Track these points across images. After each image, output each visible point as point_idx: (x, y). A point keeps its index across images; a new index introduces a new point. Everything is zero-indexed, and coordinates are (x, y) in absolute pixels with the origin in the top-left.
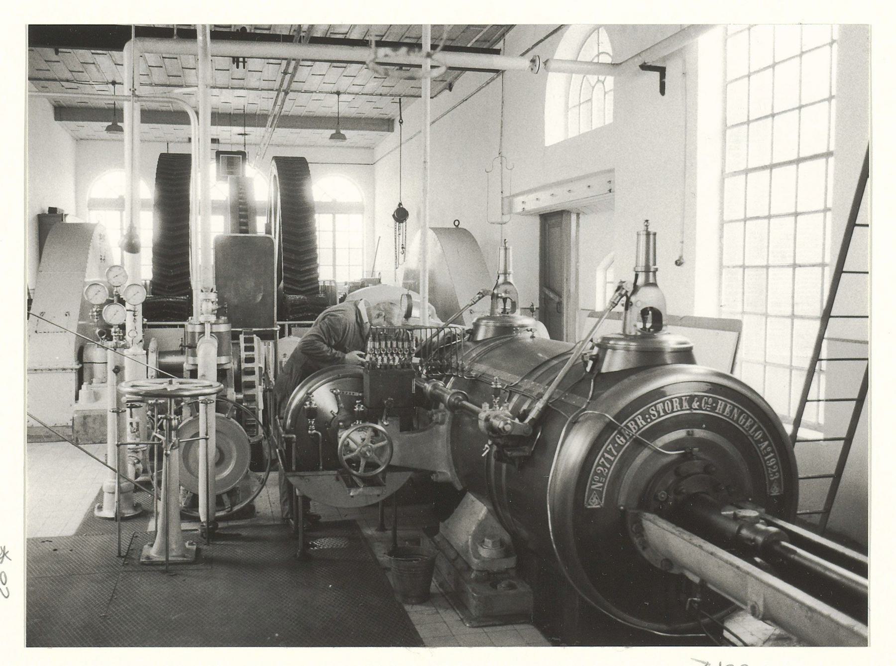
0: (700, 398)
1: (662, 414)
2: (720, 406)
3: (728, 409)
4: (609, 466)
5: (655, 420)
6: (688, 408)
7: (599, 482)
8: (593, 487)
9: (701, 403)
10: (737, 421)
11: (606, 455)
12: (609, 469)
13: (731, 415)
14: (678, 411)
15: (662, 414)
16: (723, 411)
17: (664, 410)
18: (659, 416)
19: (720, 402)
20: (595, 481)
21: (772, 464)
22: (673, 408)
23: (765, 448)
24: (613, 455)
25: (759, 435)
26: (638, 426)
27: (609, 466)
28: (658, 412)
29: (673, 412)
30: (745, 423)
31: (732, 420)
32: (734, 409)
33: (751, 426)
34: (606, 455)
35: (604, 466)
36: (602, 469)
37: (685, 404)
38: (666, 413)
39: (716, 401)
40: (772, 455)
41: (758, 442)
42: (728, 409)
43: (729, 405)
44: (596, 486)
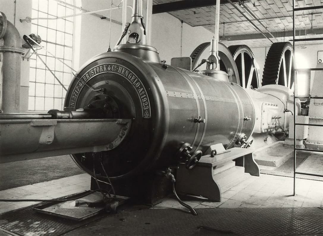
0: (111, 65)
1: (96, 73)
2: (120, 70)
3: (123, 71)
4: (76, 96)
5: (93, 76)
6: (106, 70)
7: (73, 102)
8: (71, 104)
9: (111, 68)
10: (127, 77)
11: (76, 91)
12: (76, 97)
13: (125, 74)
14: (102, 72)
15: (96, 73)
16: (121, 72)
17: (96, 71)
18: (94, 74)
19: (120, 67)
20: (72, 102)
21: (145, 101)
22: (100, 71)
23: (141, 92)
24: (78, 91)
25: (138, 85)
26: (87, 78)
27: (76, 96)
28: (94, 72)
29: (100, 72)
30: (132, 78)
31: (125, 76)
32: (126, 71)
33: (134, 80)
34: (76, 91)
35: (75, 96)
36: (74, 96)
37: (105, 68)
38: (97, 73)
39: (118, 67)
40: (145, 96)
41: (138, 88)
42: (123, 71)
43: (124, 69)
44: (72, 104)
